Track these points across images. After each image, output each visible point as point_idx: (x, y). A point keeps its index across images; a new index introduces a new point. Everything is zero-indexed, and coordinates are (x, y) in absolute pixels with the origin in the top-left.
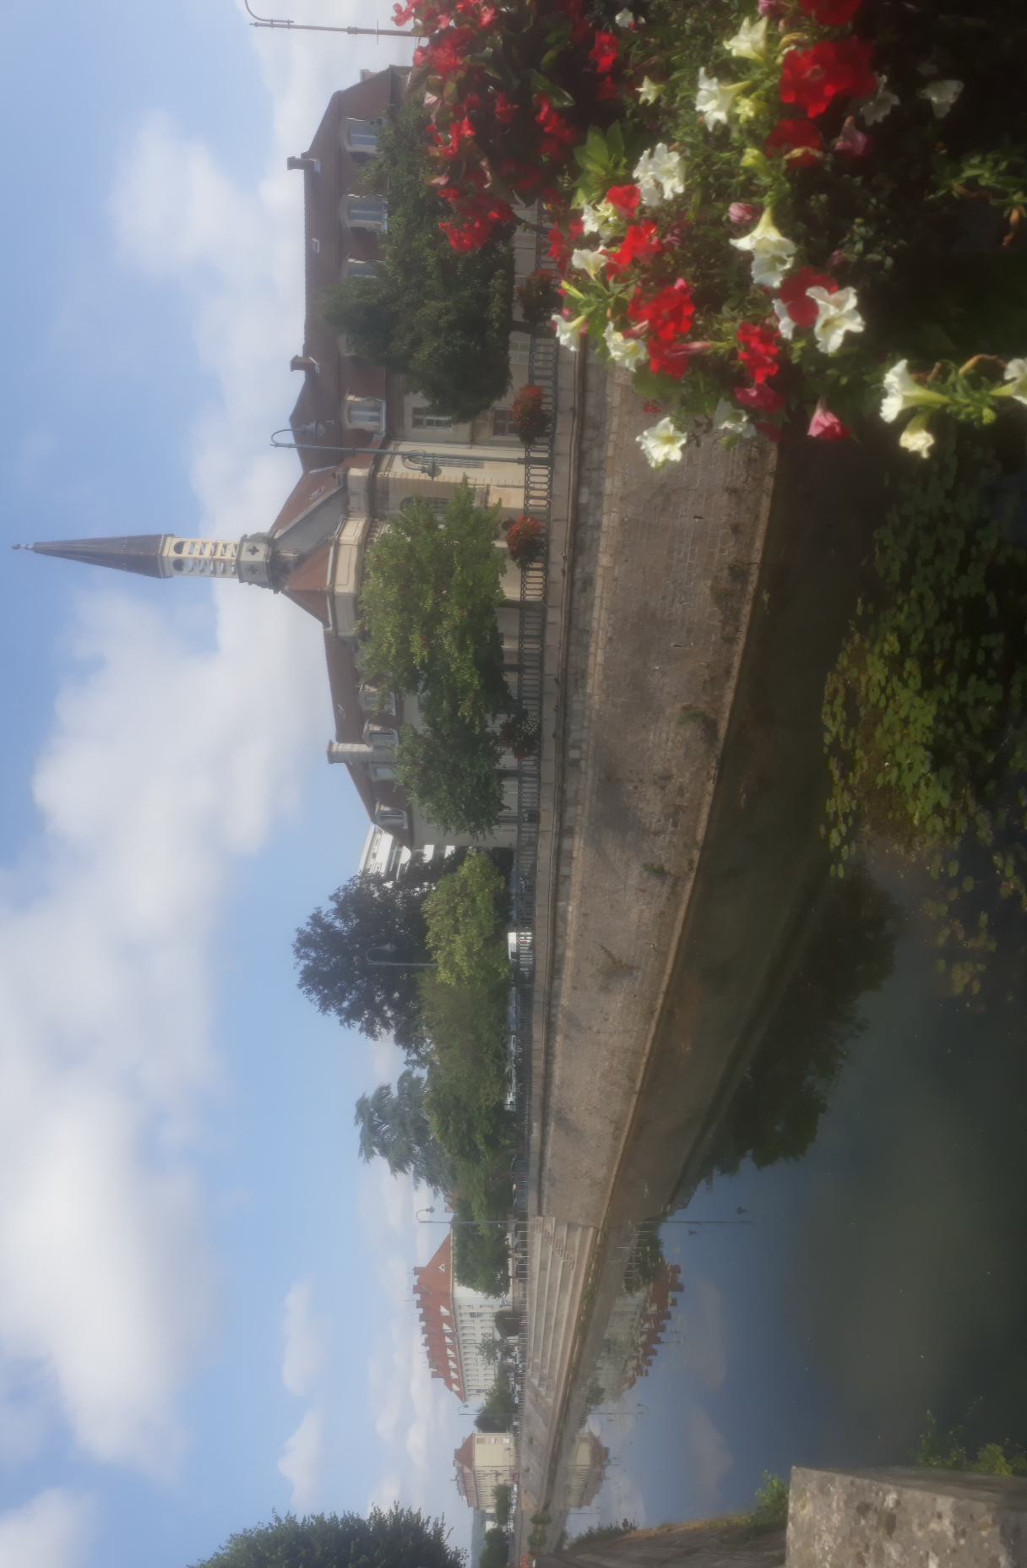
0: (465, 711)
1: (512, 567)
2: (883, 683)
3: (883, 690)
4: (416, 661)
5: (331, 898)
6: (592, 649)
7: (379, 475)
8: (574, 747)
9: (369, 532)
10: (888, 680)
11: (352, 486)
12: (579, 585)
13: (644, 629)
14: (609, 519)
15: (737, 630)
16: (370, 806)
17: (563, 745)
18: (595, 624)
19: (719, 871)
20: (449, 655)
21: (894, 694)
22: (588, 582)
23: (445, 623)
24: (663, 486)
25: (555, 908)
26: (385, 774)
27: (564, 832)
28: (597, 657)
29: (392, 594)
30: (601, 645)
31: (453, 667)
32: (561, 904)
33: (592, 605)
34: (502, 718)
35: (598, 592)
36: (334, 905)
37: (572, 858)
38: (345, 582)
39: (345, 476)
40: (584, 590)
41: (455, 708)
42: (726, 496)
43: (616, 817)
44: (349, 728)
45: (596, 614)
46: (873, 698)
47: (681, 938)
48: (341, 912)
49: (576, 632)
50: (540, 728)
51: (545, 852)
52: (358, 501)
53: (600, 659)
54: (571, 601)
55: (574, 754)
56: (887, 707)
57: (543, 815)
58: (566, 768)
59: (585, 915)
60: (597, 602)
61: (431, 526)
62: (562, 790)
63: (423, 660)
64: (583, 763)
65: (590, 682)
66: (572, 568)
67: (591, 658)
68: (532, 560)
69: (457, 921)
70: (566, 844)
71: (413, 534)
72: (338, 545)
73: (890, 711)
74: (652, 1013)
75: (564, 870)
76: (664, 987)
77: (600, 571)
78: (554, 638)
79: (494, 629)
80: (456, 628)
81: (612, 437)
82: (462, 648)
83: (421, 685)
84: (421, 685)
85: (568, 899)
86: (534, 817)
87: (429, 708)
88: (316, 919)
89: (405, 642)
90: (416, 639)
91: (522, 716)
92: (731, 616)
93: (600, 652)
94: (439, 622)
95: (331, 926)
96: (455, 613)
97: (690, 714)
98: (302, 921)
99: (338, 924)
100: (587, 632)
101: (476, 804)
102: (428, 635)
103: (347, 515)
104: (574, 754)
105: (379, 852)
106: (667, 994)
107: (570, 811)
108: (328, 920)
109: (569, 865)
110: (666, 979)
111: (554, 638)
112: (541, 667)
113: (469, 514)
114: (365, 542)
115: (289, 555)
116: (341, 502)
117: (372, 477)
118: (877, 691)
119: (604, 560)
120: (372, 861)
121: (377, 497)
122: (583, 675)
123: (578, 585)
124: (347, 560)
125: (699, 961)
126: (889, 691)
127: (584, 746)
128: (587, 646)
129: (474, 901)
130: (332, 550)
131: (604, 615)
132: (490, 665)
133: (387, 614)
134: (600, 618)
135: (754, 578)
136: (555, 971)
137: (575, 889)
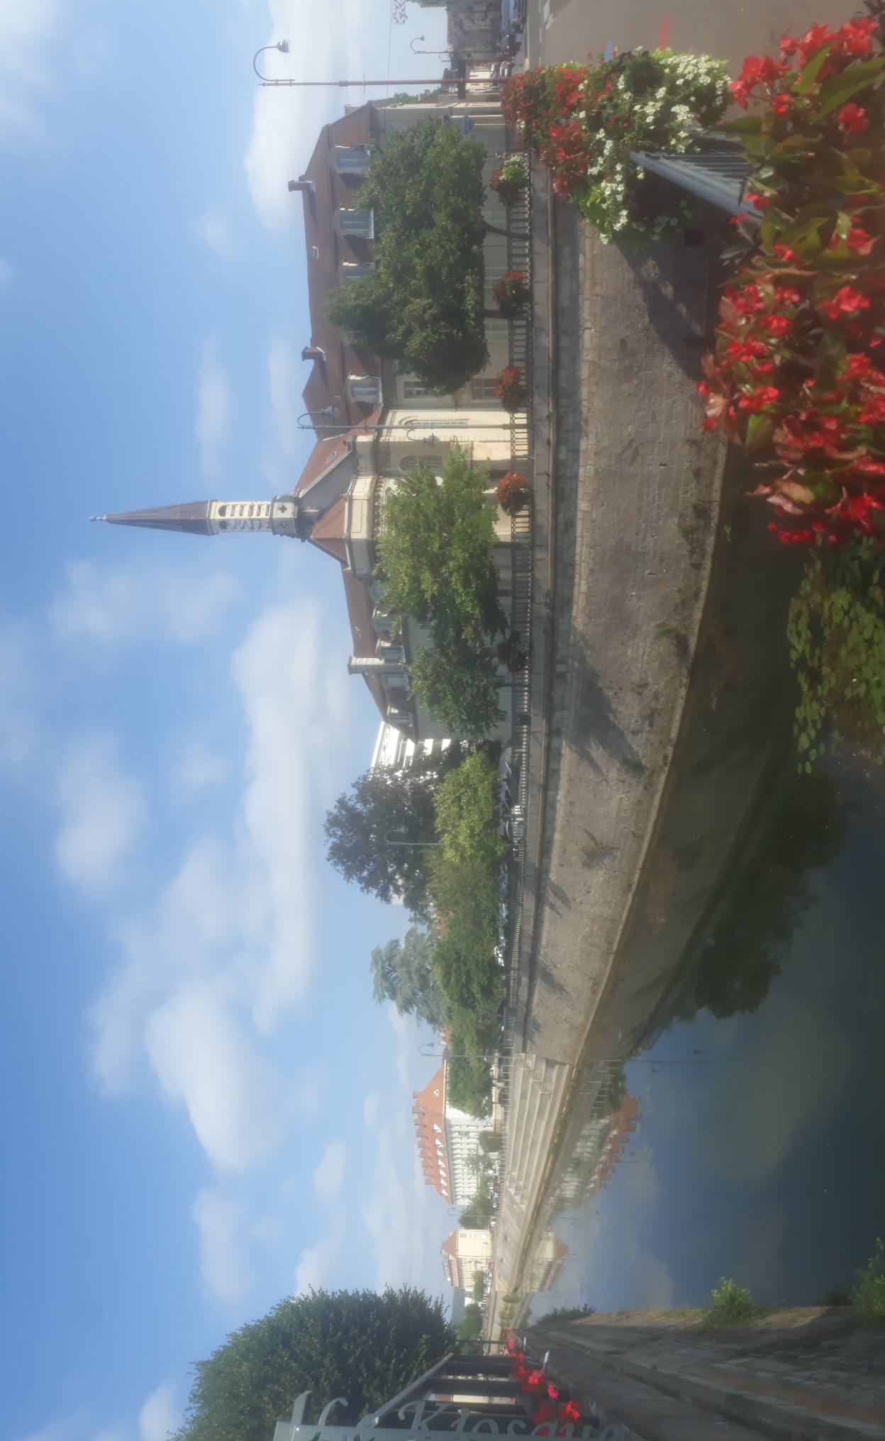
0: (467, 633)
1: (500, 511)
2: (846, 607)
3: (846, 613)
4: (428, 595)
5: (353, 786)
6: (577, 580)
7: (382, 439)
8: (563, 662)
9: (376, 487)
10: (851, 605)
11: (359, 450)
12: (561, 528)
13: (620, 561)
14: (585, 471)
15: (703, 557)
16: (383, 709)
17: (551, 661)
18: (577, 558)
19: (691, 765)
20: (456, 591)
21: (857, 617)
22: (570, 524)
23: (451, 564)
24: (632, 441)
25: (545, 798)
26: (394, 682)
27: (553, 733)
28: (581, 586)
29: (405, 542)
30: (583, 576)
31: (458, 601)
32: (550, 793)
33: (574, 543)
34: (499, 637)
35: (579, 532)
36: (355, 791)
37: (560, 755)
38: (359, 531)
39: (354, 442)
40: (566, 531)
41: (459, 631)
42: (687, 447)
43: (596, 722)
44: (363, 646)
45: (578, 550)
46: (837, 619)
47: (656, 822)
48: (362, 797)
49: (563, 567)
50: (531, 647)
51: (538, 752)
52: (365, 463)
53: (583, 588)
54: (556, 539)
55: (560, 668)
56: (850, 627)
57: (534, 719)
58: (553, 678)
59: (572, 803)
60: (579, 540)
61: (432, 484)
62: (549, 697)
63: (433, 595)
64: (569, 675)
65: (575, 608)
66: (555, 514)
67: (576, 588)
68: (520, 509)
69: (461, 808)
70: (555, 742)
71: (418, 492)
72: (351, 500)
73: (854, 631)
74: (630, 886)
75: (553, 766)
76: (640, 863)
77: (579, 515)
78: (544, 573)
79: (491, 568)
80: (460, 567)
81: (585, 403)
82: (466, 583)
83: (429, 615)
84: (429, 615)
85: (557, 789)
86: (526, 720)
87: (439, 634)
88: (342, 803)
89: (416, 580)
90: (427, 576)
91: (516, 636)
92: (696, 547)
93: (583, 583)
94: (444, 562)
95: (353, 808)
96: (458, 556)
97: (664, 632)
98: (331, 805)
99: (359, 807)
100: (572, 565)
101: (477, 713)
102: (435, 571)
103: (357, 474)
104: (560, 668)
105: (390, 748)
106: (643, 869)
107: (557, 715)
108: (351, 803)
109: (559, 761)
110: (642, 857)
111: (544, 573)
112: (532, 598)
113: (467, 473)
114: (374, 497)
115: (311, 511)
116: (351, 466)
117: (376, 441)
118: (841, 614)
119: (583, 505)
120: (383, 754)
121: (381, 460)
122: (569, 602)
123: (564, 527)
124: (360, 513)
125: (673, 841)
126: (852, 614)
127: (570, 661)
128: (572, 578)
129: (475, 790)
130: (347, 504)
131: (585, 549)
132: (488, 596)
133: (400, 558)
134: (582, 554)
135: (715, 513)
136: (545, 848)
137: (563, 782)
